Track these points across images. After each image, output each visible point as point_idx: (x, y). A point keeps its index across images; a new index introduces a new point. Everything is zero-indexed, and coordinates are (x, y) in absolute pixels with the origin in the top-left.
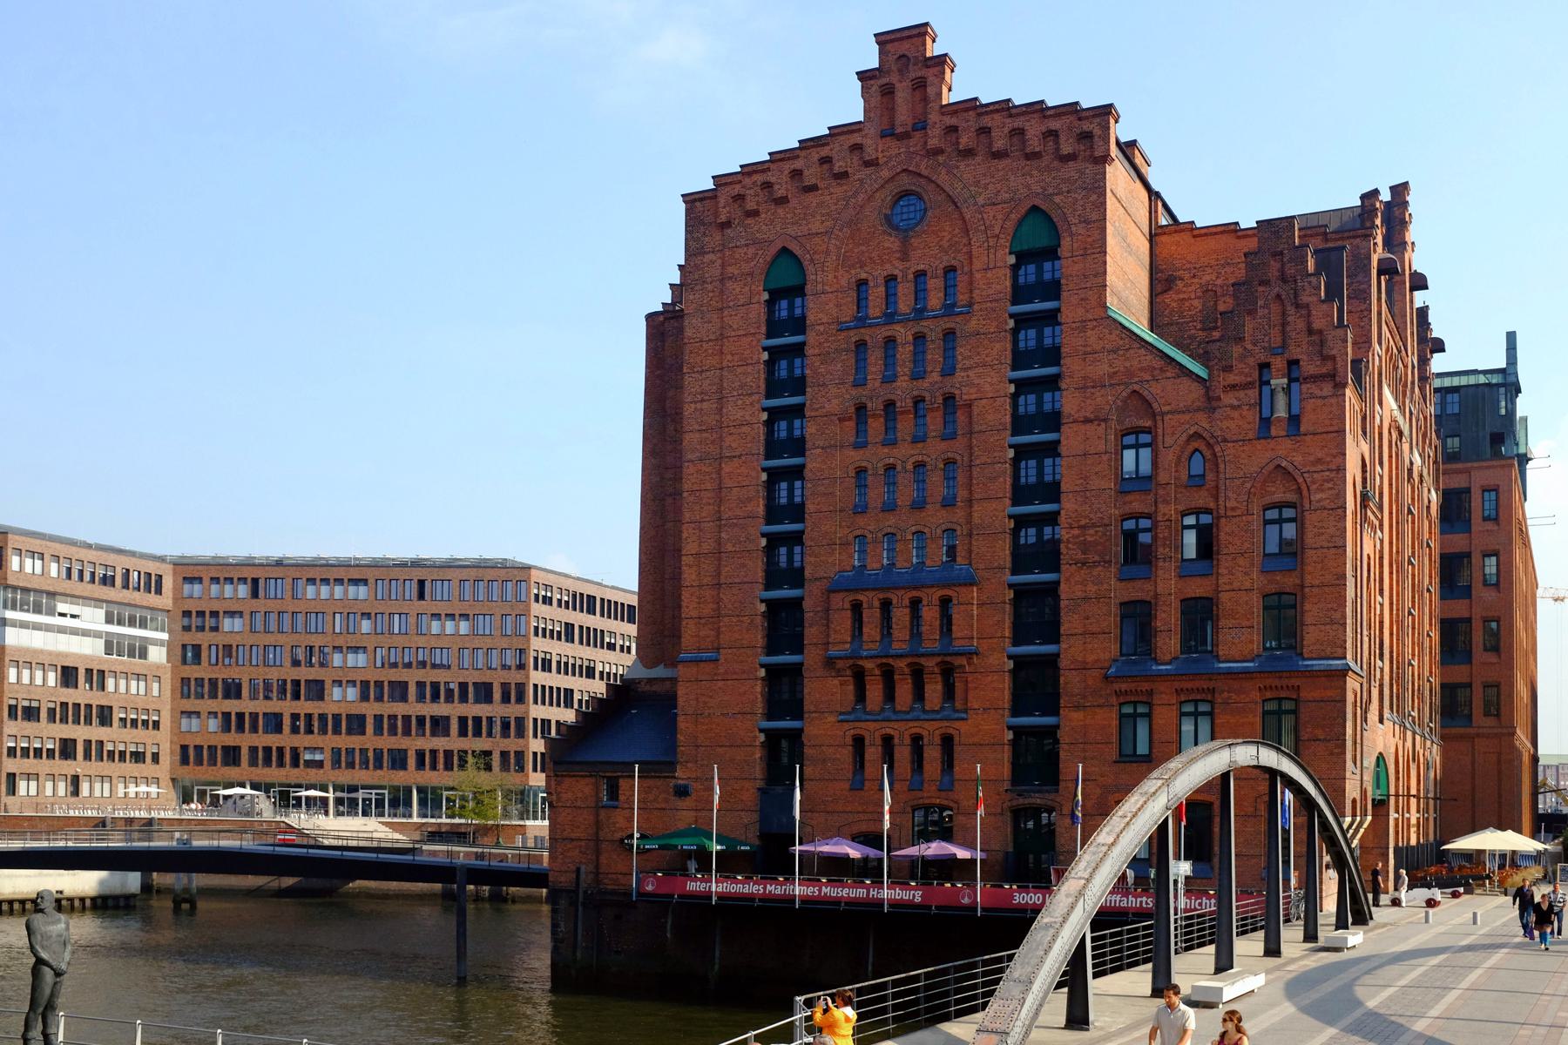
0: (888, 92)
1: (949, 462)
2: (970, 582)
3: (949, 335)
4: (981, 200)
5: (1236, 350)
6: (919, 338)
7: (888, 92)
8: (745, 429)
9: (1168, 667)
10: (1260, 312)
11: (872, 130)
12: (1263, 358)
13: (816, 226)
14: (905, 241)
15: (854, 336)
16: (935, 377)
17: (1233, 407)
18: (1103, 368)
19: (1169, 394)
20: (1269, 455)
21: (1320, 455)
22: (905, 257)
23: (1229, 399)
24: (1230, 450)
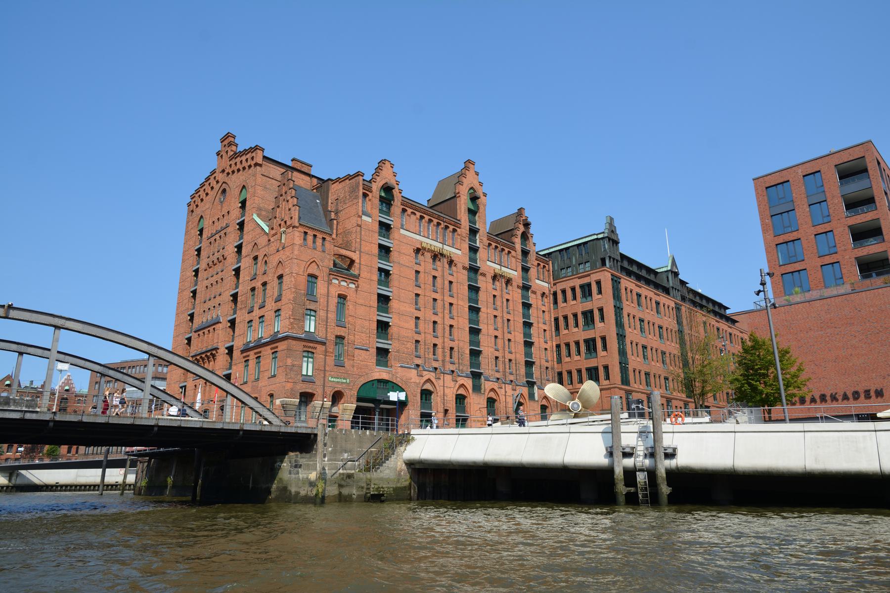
2: (219, 322)
4: (235, 187)
5: (275, 221)
13: (207, 207)
14: (222, 206)
19: (262, 241)
22: (221, 212)
24: (271, 258)
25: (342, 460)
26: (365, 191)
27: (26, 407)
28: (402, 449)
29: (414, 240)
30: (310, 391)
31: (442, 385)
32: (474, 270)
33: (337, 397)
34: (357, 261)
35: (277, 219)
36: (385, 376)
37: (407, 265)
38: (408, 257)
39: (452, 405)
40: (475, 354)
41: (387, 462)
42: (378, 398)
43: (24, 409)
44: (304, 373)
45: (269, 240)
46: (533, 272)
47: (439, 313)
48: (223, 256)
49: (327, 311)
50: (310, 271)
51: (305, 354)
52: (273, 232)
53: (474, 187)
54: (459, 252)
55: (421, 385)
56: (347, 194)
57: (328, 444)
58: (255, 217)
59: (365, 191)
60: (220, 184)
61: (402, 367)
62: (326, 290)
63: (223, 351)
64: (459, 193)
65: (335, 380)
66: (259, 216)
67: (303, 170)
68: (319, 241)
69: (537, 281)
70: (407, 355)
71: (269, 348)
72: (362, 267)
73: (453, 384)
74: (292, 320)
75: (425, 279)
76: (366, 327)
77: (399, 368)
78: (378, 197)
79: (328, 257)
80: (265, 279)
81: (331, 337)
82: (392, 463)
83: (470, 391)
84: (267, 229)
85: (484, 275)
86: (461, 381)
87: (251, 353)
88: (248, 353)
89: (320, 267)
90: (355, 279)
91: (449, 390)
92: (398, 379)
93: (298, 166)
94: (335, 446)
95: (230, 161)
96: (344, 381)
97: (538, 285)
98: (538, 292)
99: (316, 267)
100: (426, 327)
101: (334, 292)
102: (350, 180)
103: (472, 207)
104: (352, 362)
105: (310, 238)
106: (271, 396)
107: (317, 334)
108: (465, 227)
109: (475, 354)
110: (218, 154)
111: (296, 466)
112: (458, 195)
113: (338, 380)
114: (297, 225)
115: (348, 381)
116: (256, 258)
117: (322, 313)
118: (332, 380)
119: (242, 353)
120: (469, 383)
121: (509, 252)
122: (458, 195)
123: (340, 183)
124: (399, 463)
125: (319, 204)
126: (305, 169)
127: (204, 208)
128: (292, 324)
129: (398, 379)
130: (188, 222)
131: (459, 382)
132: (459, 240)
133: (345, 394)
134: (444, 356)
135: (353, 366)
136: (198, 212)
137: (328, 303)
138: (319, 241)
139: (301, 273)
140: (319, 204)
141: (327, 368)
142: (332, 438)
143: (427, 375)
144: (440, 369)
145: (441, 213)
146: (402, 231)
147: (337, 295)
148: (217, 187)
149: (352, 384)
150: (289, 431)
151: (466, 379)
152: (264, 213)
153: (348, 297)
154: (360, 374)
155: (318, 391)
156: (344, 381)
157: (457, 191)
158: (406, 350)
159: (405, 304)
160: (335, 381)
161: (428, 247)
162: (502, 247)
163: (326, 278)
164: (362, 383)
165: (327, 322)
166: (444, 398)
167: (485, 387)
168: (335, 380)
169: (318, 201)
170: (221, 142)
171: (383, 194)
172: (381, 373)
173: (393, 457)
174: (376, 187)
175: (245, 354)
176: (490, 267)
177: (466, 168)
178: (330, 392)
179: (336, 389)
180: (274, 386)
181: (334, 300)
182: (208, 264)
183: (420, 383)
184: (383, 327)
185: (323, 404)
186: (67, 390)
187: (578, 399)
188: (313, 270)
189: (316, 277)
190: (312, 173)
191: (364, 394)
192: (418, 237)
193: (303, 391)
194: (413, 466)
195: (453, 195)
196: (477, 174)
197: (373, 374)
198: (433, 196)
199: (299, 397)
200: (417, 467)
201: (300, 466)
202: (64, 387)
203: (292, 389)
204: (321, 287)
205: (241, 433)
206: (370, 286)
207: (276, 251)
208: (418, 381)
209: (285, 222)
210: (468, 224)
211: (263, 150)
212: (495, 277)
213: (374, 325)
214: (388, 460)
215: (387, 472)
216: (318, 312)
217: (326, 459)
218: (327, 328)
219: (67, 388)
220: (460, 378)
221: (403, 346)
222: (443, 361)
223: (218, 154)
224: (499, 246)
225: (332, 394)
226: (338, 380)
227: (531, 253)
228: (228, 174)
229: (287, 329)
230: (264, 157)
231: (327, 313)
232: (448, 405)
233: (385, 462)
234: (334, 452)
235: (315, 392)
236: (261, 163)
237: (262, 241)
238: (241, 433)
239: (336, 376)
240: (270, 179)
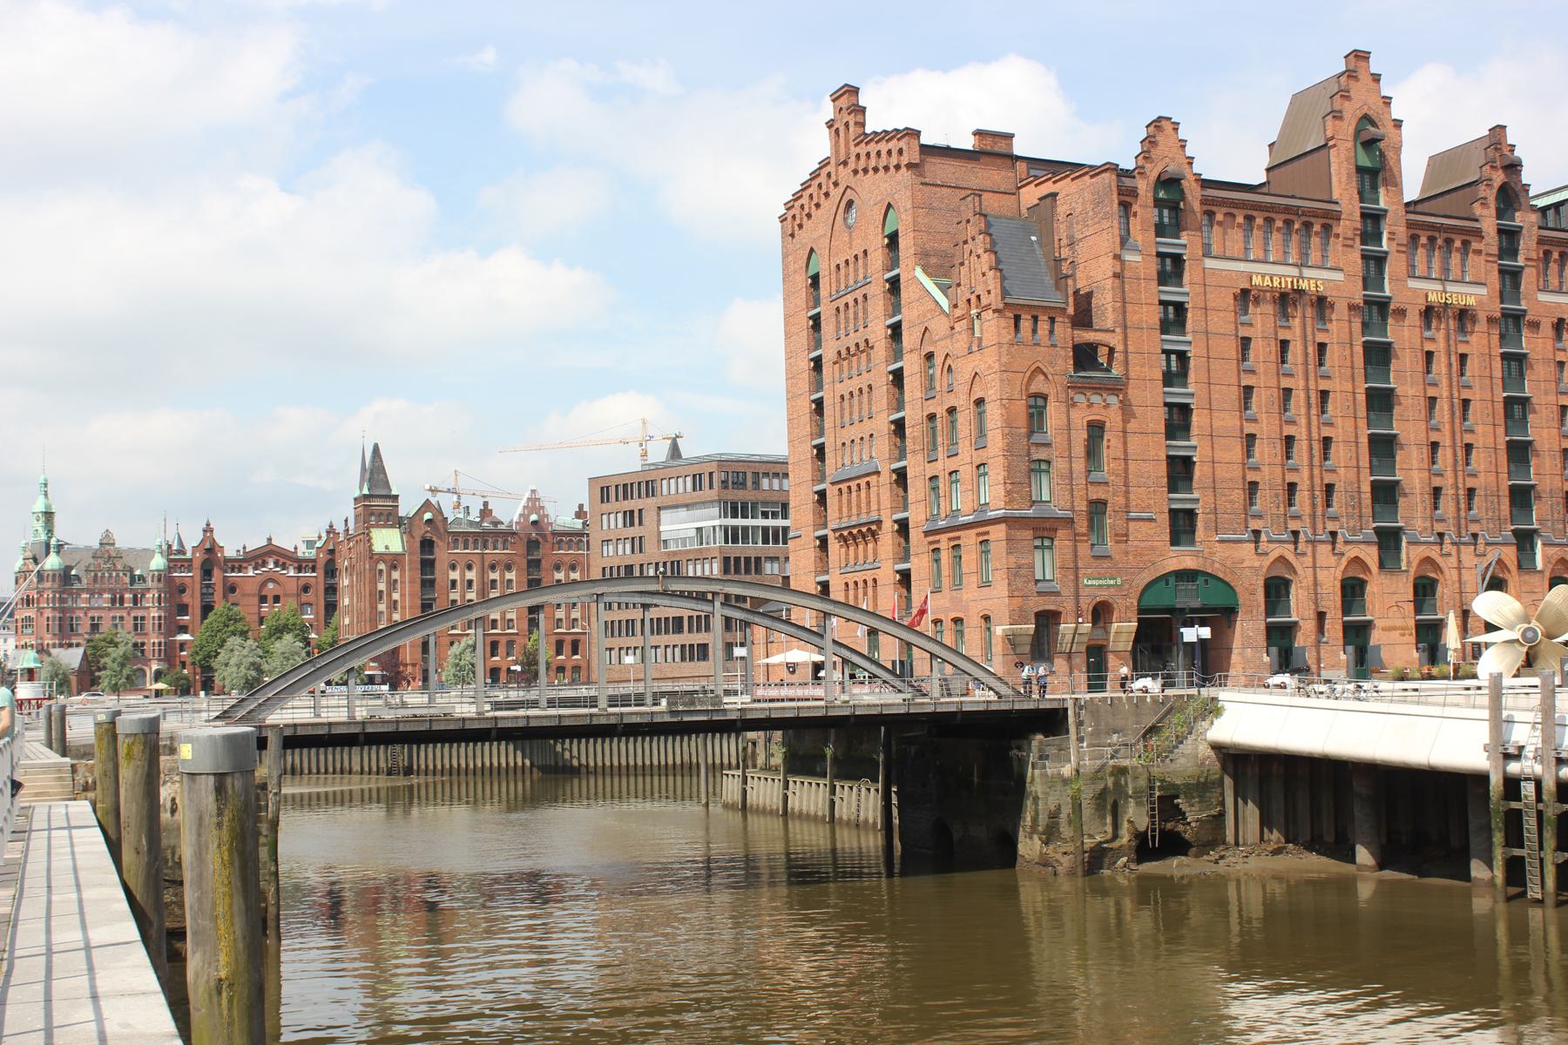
0: (837, 131)
1: (870, 387)
3: (865, 296)
4: (872, 203)
6: (856, 301)
7: (837, 131)
8: (804, 374)
9: (971, 517)
10: (966, 262)
11: (833, 161)
12: (968, 296)
15: (835, 304)
16: (861, 329)
17: (960, 333)
18: (916, 313)
19: (939, 326)
20: (972, 365)
21: (990, 362)
22: (850, 248)
23: (958, 327)
25: (1110, 745)
26: (1123, 198)
27: (712, 705)
28: (1205, 724)
29: (1234, 274)
30: (1052, 607)
31: (1310, 564)
32: (1377, 309)
33: (1101, 613)
34: (1119, 348)
35: (962, 287)
36: (1189, 563)
37: (1222, 331)
38: (1221, 314)
39: (1332, 602)
40: (1385, 494)
41: (1181, 746)
42: (1178, 606)
43: (710, 708)
45: (952, 328)
46: (1528, 279)
47: (1297, 419)
48: (867, 341)
49: (1070, 457)
50: (1033, 389)
51: (1038, 543)
52: (958, 312)
53: (1370, 113)
54: (1339, 276)
55: (1264, 570)
56: (1089, 207)
57: (1087, 722)
58: (919, 273)
59: (1123, 198)
60: (841, 189)
61: (1222, 541)
62: (1064, 417)
63: (888, 527)
64: (1332, 138)
65: (1094, 582)
66: (925, 271)
67: (996, 149)
68: (1043, 326)
69: (1543, 297)
70: (1233, 516)
71: (973, 532)
72: (1131, 357)
73: (1333, 560)
74: (1009, 487)
75: (1262, 351)
76: (1146, 475)
77: (1217, 545)
78: (1150, 202)
80: (951, 401)
81: (1082, 506)
82: (1189, 747)
83: (1374, 567)
84: (944, 303)
85: (1401, 313)
86: (1352, 552)
87: (944, 537)
88: (937, 538)
89: (1050, 377)
90: (1117, 387)
91: (1326, 572)
92: (1217, 565)
93: (988, 145)
94: (1097, 725)
95: (856, 145)
96: (1112, 582)
97: (1544, 304)
98: (1543, 320)
99: (1043, 377)
100: (1267, 451)
101: (1080, 418)
102: (1092, 177)
103: (1365, 161)
104: (1123, 546)
105: (1026, 324)
106: (987, 618)
108: (1351, 214)
109: (1385, 494)
110: (830, 124)
111: (1041, 758)
112: (1331, 143)
113: (1101, 582)
114: (1001, 306)
115: (1119, 581)
116: (930, 356)
117: (1059, 465)
118: (1090, 583)
119: (926, 536)
120: (1371, 555)
121: (1466, 243)
122: (1331, 143)
123: (1073, 180)
124: (1201, 747)
125: (1036, 246)
126: (1000, 147)
127: (814, 232)
128: (1008, 493)
129: (1217, 565)
130: (785, 256)
131: (1347, 555)
133: (1115, 606)
134: (1314, 506)
135: (1127, 553)
136: (805, 237)
137: (1070, 444)
138: (1043, 326)
139: (1016, 396)
140: (1036, 246)
141: (1080, 565)
142: (1092, 712)
143: (1276, 551)
144: (1305, 533)
145: (1293, 197)
146: (1210, 263)
147: (1085, 424)
148: (835, 193)
149: (1127, 586)
150: (1026, 707)
151: (1362, 546)
152: (935, 261)
153: (1108, 424)
154: (1141, 565)
155: (1066, 605)
156: (1112, 582)
157: (1329, 134)
158: (1229, 506)
160: (1095, 586)
161: (1267, 282)
162: (1445, 235)
163: (1062, 396)
164: (1146, 581)
165: (1071, 479)
166: (1315, 589)
167: (1408, 558)
168: (1094, 582)
169: (1034, 238)
170: (834, 101)
171: (1161, 195)
172: (1181, 559)
173: (1191, 738)
174: (1144, 186)
175: (931, 539)
176: (1414, 290)
177: (1350, 74)
178: (1087, 605)
179: (1098, 599)
180: (990, 602)
181: (1080, 436)
182: (839, 353)
183: (1261, 566)
184: (1180, 471)
185: (1076, 628)
186: (535, 523)
187: (1537, 620)
188: (1039, 385)
189: (1045, 397)
190: (1017, 151)
191: (1150, 601)
192: (1242, 266)
193: (1041, 609)
194: (1225, 751)
195: (1322, 143)
196: (1376, 78)
197: (1166, 562)
198: (1281, 135)
199: (1033, 621)
200: (1231, 752)
201: (1047, 757)
202: (529, 515)
203: (1021, 609)
204: (1054, 415)
205: (959, 715)
206: (1149, 397)
207: (967, 352)
208: (1257, 564)
209: (978, 297)
210: (1358, 205)
211: (917, 134)
212: (1429, 313)
213: (1162, 469)
214: (1182, 743)
215: (1182, 760)
216: (1054, 464)
217: (1085, 744)
218: (1072, 490)
219: (534, 517)
220: (1349, 547)
221: (1224, 499)
222: (1313, 516)
223: (830, 124)
224: (1437, 235)
225: (1091, 608)
226: (1101, 582)
227: (1524, 231)
228: (855, 172)
229: (1003, 503)
230: (923, 147)
231: (1071, 462)
232: (1323, 603)
233: (1177, 747)
234: (1096, 733)
235: (1061, 609)
236: (917, 161)
237: (939, 326)
238: (959, 715)
239: (1097, 576)
240: (938, 189)
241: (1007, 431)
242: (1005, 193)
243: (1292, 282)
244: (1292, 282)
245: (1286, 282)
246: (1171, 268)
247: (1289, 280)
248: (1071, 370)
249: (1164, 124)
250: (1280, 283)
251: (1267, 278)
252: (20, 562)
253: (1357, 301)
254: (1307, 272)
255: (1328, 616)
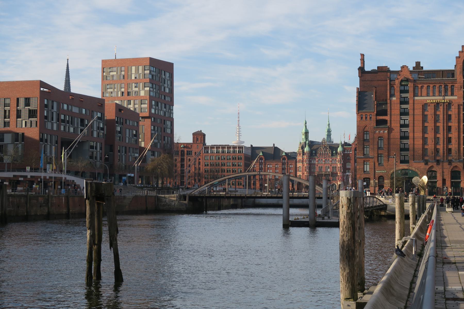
29: (423, 100)
34: (389, 120)
37: (418, 114)
38: (418, 110)
44: (365, 170)
54: (456, 98)
73: (448, 166)
79: (373, 122)
107: (370, 154)
115: (386, 171)
132: (457, 90)
147: (378, 137)
151: (458, 163)
155: (372, 176)
158: (417, 154)
159: (417, 133)
161: (432, 101)
193: (365, 177)
225: (378, 177)
240: (366, 82)
241: (358, 139)
242: (384, 81)
243: (439, 101)
244: (439, 101)
245: (437, 101)
246: (404, 102)
247: (438, 100)
248: (375, 125)
249: (405, 68)
250: (436, 101)
251: (432, 100)
252: (298, 149)
253: (461, 103)
254: (446, 97)
255: (446, 180)
